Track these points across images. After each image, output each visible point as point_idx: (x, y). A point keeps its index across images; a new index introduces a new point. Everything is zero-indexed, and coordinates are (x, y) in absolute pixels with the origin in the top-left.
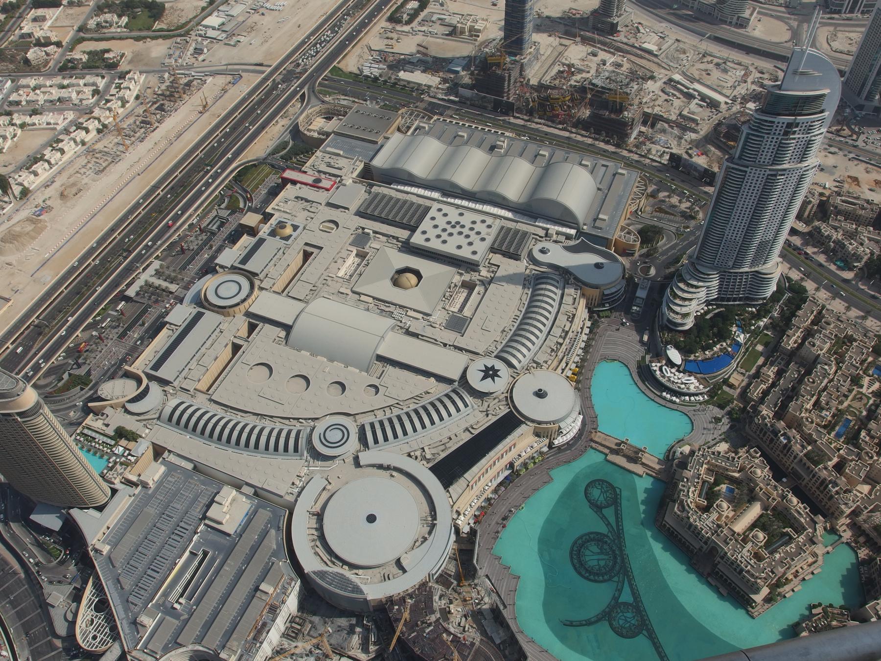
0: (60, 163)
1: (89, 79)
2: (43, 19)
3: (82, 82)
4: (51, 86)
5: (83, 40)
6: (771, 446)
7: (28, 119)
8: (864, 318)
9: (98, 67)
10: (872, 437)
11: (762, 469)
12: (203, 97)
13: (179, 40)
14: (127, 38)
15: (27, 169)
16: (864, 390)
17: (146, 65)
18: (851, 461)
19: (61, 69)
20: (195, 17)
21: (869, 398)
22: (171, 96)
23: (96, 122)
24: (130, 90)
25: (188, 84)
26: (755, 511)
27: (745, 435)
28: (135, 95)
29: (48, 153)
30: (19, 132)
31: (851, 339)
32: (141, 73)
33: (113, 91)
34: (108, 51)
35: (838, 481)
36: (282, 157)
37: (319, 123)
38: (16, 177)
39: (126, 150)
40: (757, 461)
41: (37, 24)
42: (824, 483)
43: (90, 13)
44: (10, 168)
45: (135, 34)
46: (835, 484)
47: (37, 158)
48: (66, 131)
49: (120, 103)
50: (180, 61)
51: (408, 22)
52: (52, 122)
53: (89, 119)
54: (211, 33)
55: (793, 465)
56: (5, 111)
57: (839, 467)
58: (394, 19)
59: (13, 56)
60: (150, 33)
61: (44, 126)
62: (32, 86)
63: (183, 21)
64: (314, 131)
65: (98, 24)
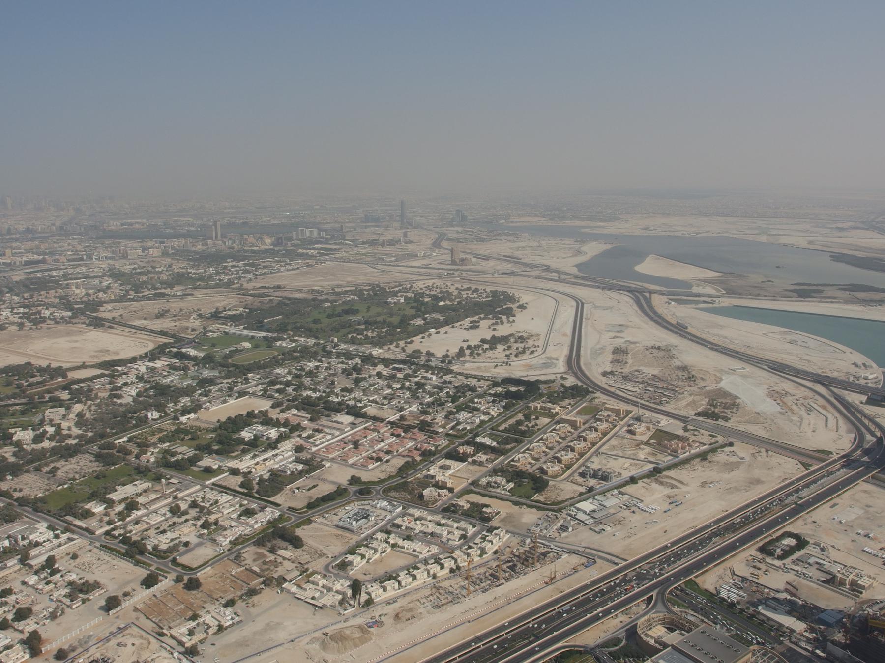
0: (408, 587)
1: (463, 524)
2: (448, 468)
3: (455, 525)
4: (430, 521)
5: (472, 492)
7: (400, 542)
9: (474, 517)
12: (553, 570)
13: (550, 513)
14: (507, 500)
15: (380, 583)
17: (514, 526)
19: (445, 510)
20: (571, 499)
22: (527, 560)
23: (453, 562)
24: (492, 544)
25: (544, 554)
28: (494, 549)
29: (402, 575)
30: (389, 549)
32: (507, 532)
33: (478, 540)
34: (487, 506)
36: (610, 653)
37: (659, 631)
38: (369, 586)
39: (468, 595)
41: (441, 470)
43: (486, 473)
44: (368, 577)
45: (515, 499)
47: (391, 576)
48: (426, 562)
49: (479, 552)
50: (545, 532)
51: (781, 558)
52: (418, 550)
53: (448, 558)
54: (581, 516)
56: (387, 530)
58: (766, 550)
59: (413, 489)
60: (528, 502)
61: (410, 551)
62: (416, 517)
63: (559, 499)
64: (652, 637)
65: (489, 484)
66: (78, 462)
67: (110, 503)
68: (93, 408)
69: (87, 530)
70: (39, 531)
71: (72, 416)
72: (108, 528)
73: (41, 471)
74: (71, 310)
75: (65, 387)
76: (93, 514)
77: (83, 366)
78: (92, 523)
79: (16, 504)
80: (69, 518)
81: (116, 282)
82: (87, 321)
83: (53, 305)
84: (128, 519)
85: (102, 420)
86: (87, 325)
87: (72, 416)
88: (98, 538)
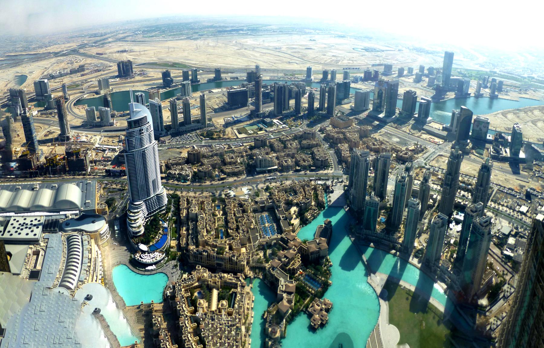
6: (203, 261)
8: (202, 193)
10: (233, 229)
11: (205, 272)
16: (219, 216)
18: (233, 243)
21: (222, 218)
26: (215, 293)
27: (190, 265)
31: (202, 203)
35: (234, 254)
40: (202, 271)
42: (230, 259)
46: (234, 256)
55: (216, 262)
57: (231, 249)
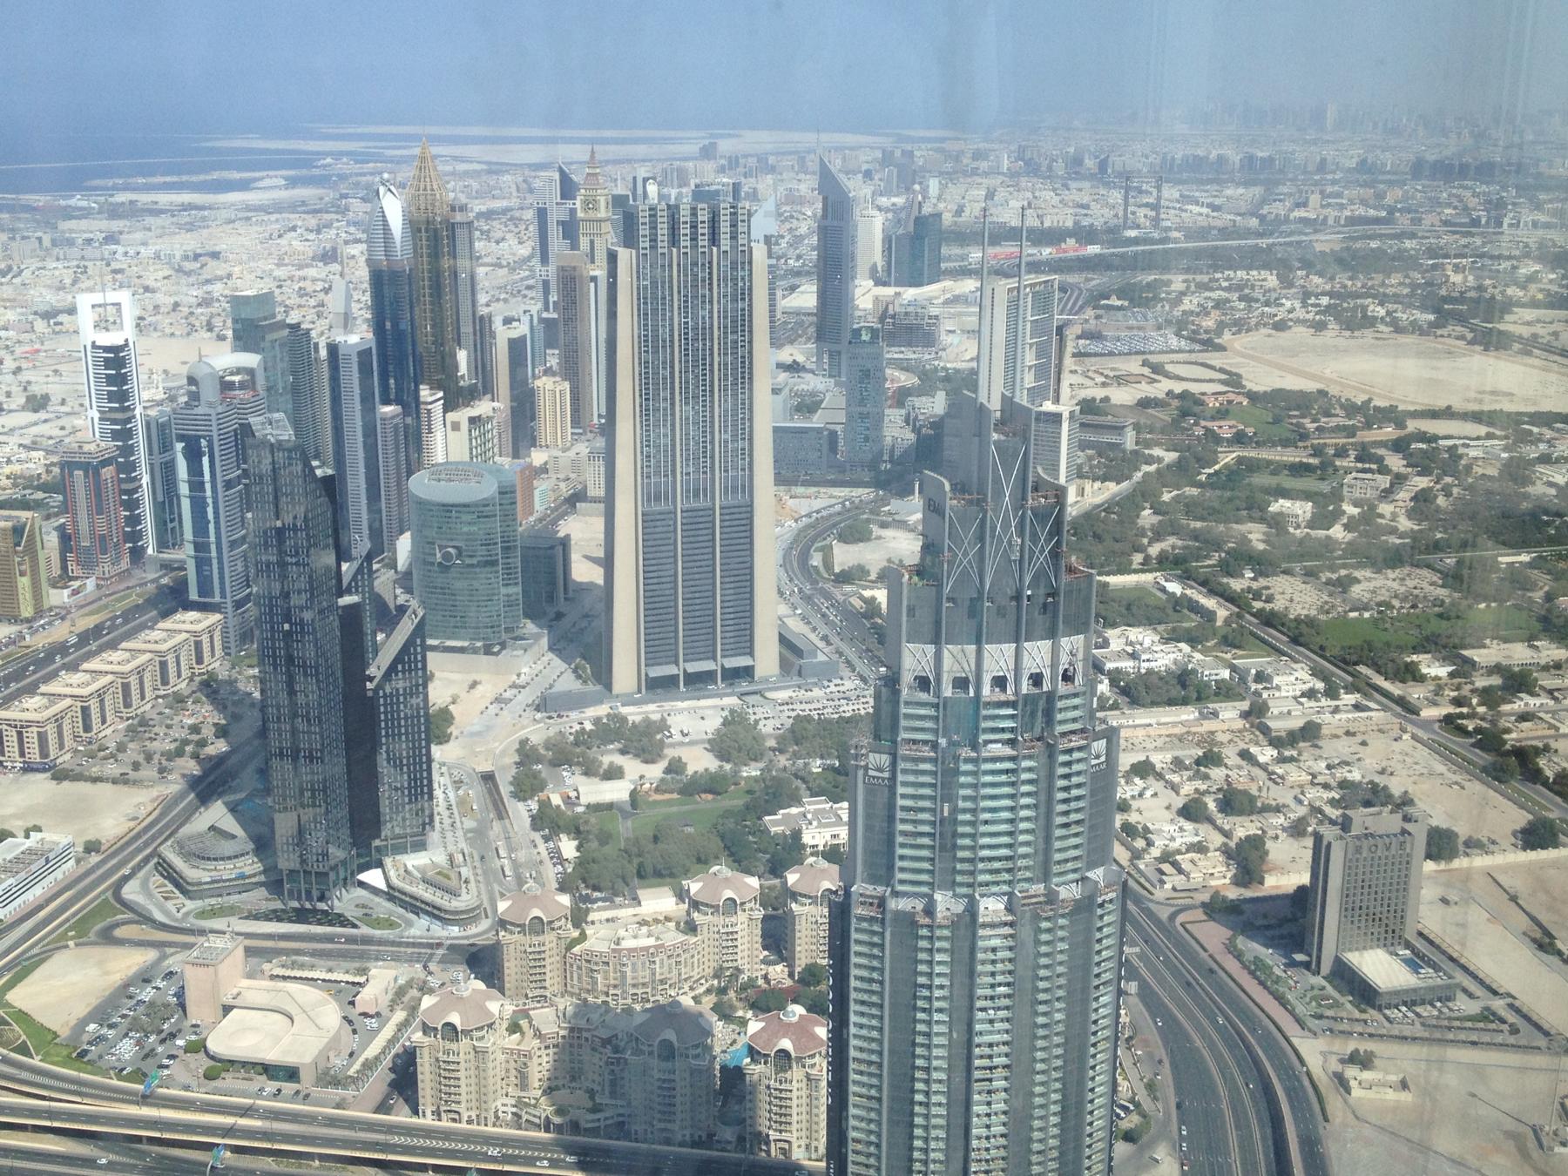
66: (1403, 579)
67: (1465, 668)
68: (1455, 491)
69: (1401, 702)
70: (1297, 674)
71: (1404, 495)
72: (1452, 710)
73: (1318, 578)
74: (1437, 311)
75: (1399, 446)
76: (1420, 679)
77: (1447, 413)
78: (1416, 693)
79: (1255, 621)
80: (1362, 669)
81: (1553, 270)
82: (1470, 336)
83: (1396, 298)
84: (1506, 708)
85: (1472, 518)
86: (1470, 343)
87: (1404, 495)
88: (1426, 725)
